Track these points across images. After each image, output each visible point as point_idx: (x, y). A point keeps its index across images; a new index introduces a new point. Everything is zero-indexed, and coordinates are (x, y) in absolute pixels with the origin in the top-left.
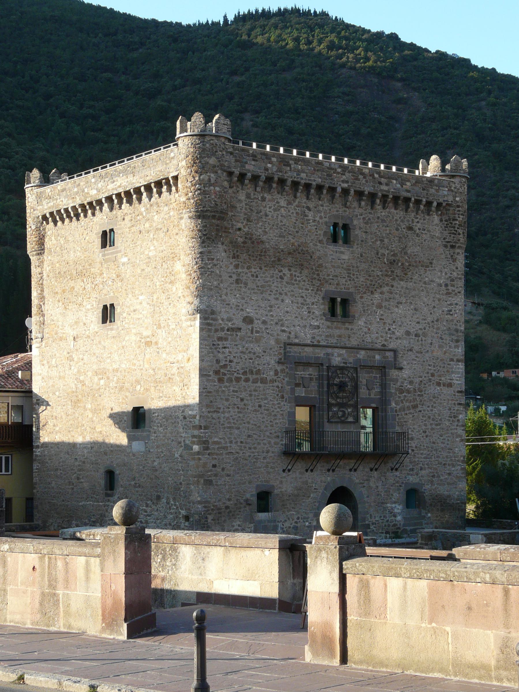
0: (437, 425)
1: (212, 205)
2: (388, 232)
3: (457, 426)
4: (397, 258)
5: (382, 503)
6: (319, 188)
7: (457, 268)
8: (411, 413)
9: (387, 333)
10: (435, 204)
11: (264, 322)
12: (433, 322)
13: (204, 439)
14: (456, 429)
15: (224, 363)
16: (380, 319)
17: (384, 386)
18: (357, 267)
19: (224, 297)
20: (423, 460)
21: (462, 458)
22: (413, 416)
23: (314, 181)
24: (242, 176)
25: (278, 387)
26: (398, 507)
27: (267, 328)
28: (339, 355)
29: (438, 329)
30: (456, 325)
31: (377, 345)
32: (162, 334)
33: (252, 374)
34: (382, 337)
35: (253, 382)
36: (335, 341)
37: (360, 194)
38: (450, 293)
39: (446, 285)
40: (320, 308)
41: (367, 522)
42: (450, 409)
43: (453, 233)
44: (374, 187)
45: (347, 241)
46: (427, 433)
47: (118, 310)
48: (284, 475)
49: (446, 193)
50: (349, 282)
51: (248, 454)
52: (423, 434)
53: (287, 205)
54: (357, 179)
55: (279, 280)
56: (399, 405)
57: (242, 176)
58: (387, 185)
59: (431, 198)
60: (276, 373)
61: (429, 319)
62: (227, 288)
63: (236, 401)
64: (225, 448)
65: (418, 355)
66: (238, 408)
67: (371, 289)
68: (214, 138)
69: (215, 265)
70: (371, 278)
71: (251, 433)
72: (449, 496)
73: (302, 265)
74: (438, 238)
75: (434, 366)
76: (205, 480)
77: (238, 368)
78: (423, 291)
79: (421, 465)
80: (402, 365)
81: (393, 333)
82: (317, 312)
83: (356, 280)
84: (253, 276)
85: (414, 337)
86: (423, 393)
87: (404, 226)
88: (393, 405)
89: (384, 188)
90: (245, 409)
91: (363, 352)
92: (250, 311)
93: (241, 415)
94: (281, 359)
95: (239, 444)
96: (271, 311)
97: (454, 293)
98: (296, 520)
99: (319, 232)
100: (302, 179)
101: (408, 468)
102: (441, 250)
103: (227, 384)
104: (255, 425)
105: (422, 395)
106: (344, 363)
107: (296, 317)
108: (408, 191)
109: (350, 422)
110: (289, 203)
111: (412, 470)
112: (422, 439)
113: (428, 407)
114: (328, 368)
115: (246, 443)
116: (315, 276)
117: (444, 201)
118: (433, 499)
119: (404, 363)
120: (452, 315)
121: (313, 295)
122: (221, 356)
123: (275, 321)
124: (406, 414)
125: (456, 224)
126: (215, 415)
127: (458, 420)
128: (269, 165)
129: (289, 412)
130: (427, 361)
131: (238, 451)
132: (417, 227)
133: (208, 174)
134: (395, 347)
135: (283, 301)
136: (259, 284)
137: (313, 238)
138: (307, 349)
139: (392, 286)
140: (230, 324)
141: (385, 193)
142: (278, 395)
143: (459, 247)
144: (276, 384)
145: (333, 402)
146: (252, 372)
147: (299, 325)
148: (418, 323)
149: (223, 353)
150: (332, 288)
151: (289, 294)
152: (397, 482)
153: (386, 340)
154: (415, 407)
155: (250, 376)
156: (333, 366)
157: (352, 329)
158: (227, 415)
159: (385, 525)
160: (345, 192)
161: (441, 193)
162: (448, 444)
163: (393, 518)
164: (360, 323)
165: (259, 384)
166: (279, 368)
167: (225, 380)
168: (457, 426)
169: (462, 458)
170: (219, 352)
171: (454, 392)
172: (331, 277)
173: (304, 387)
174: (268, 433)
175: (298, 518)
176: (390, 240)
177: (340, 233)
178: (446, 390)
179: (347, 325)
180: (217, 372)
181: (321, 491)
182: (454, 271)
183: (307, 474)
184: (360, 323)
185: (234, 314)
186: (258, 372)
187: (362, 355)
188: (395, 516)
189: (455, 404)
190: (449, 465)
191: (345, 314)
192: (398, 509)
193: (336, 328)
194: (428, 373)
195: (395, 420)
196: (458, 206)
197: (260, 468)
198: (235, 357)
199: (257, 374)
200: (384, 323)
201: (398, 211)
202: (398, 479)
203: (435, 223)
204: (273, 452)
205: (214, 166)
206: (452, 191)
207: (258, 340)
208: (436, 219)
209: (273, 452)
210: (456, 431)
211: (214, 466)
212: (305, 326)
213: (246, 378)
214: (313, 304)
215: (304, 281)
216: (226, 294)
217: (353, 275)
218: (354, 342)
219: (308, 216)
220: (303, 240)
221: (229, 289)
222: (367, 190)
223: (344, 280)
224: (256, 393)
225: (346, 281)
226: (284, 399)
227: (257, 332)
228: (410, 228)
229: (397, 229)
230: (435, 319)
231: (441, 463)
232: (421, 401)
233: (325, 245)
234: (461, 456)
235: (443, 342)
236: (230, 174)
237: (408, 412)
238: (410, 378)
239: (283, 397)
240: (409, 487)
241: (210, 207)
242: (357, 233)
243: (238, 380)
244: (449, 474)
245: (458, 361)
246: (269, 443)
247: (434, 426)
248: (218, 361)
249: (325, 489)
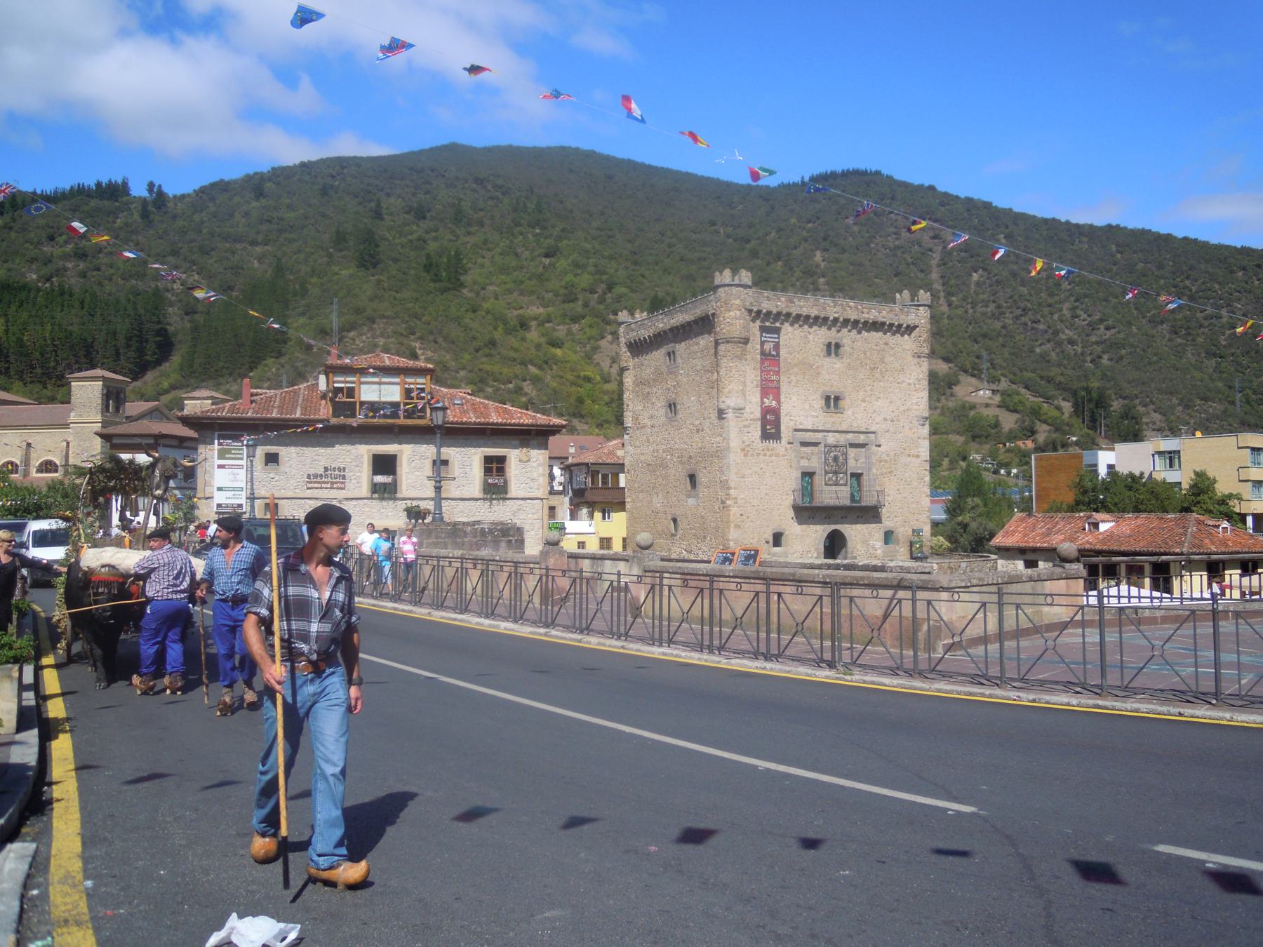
6: (817, 318)
17: (868, 458)
24: (759, 312)
32: (707, 422)
37: (846, 321)
45: (837, 355)
47: (678, 407)
61: (902, 409)
89: (866, 316)
102: (911, 359)
119: (882, 441)
150: (828, 389)
160: (836, 320)
177: (833, 349)
180: (743, 450)
186: (773, 449)
187: (850, 436)
191: (836, 406)
218: (844, 427)
236: (750, 311)
242: (846, 349)
243: (758, 454)
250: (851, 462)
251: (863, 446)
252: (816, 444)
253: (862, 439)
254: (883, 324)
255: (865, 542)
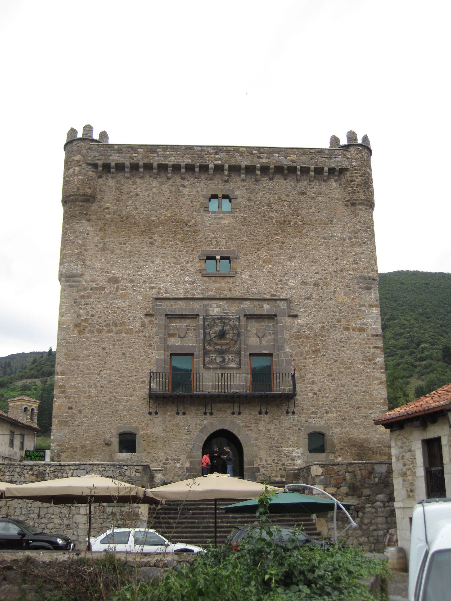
0: (346, 368)
1: (74, 190)
2: (276, 198)
3: (374, 368)
4: (289, 219)
5: (276, 447)
7: (360, 222)
8: (311, 358)
9: (277, 284)
10: (326, 169)
11: (131, 281)
12: (335, 272)
13: (61, 384)
14: (373, 372)
15: (85, 317)
16: (269, 272)
18: (240, 229)
19: (88, 262)
20: (329, 403)
21: (382, 401)
22: (314, 361)
23: (183, 162)
25: (145, 337)
26: (296, 449)
27: (134, 286)
28: (218, 306)
29: (344, 277)
30: (362, 272)
31: (265, 296)
33: (117, 326)
34: (271, 288)
35: (117, 333)
36: (213, 293)
38: (354, 245)
39: (350, 239)
40: (193, 265)
41: (255, 466)
42: (363, 353)
43: (352, 192)
44: (252, 161)
46: (334, 377)
48: (150, 417)
49: (339, 160)
50: (230, 242)
51: (108, 398)
52: (328, 378)
53: (160, 185)
54: (233, 156)
55: (149, 245)
56: (295, 350)
57: (107, 167)
58: (267, 158)
59: (320, 165)
60: (143, 324)
61: (331, 269)
62: (92, 256)
63: (95, 349)
64: (85, 392)
65: (318, 303)
66: (99, 356)
67: (257, 247)
68: (79, 142)
69: (77, 237)
70: (257, 238)
71: (112, 378)
72: (366, 440)
73: (176, 232)
74: (337, 199)
75: (340, 313)
76: (59, 421)
77: (100, 321)
78: (321, 245)
79: (327, 408)
80: (296, 313)
81: (286, 284)
82: (191, 270)
83: (238, 240)
84: (120, 243)
85: (312, 287)
86: (327, 338)
87: (296, 192)
88: (288, 349)
89: (265, 161)
90: (106, 357)
91: (248, 303)
92: (116, 272)
93: (103, 363)
94: (149, 312)
95: (99, 388)
96: (139, 271)
97: (358, 244)
98: (164, 461)
99: (195, 204)
100: (170, 161)
101: (309, 412)
102: (341, 208)
103: (88, 335)
104: (118, 371)
105: (326, 340)
106: (224, 313)
107: (167, 275)
108: (292, 161)
109: (232, 368)
110: (163, 184)
111: (315, 413)
112: (327, 383)
113: (334, 351)
114: (205, 318)
115: (107, 388)
116: (190, 240)
117: (338, 166)
118: (344, 442)
119: (301, 311)
120: (357, 264)
121: (188, 255)
122: (82, 311)
123: (143, 279)
124: (306, 359)
125: (354, 184)
126: (73, 363)
127: (375, 363)
128: (135, 155)
129: (157, 359)
130: (330, 308)
131: (97, 395)
132: (310, 192)
133: (74, 168)
134: (288, 296)
135: (152, 262)
136: (127, 249)
137: (188, 208)
138: (179, 302)
139: (283, 243)
140: (93, 285)
141: (265, 165)
142: (144, 344)
143: (360, 204)
144: (141, 334)
145: (211, 348)
146: (116, 325)
147: (171, 282)
148: (317, 273)
149: (85, 309)
151: (160, 256)
152: (295, 426)
153: (276, 291)
154: (318, 351)
155: (113, 328)
156: (212, 316)
157: (233, 283)
158: (86, 362)
159: (280, 469)
161: (333, 160)
162: (362, 387)
163: (292, 462)
164: (243, 276)
165: (123, 335)
166: (147, 320)
167: (86, 332)
168: (374, 368)
169: (382, 401)
170: (80, 308)
171: (368, 335)
172: (209, 240)
173: (180, 337)
174: (132, 379)
175: (167, 459)
176: (279, 205)
178: (355, 334)
179: (227, 279)
180: (77, 325)
181: (196, 434)
182: (356, 224)
183: (179, 416)
184: (243, 276)
185: (98, 276)
186: (123, 324)
187: (246, 305)
188: (293, 460)
189: (369, 347)
190: (365, 408)
192: (297, 453)
193: (214, 282)
194: (332, 319)
195: (290, 364)
196: (355, 170)
197: (122, 410)
198: (97, 312)
199: (121, 325)
200: (274, 276)
201: (288, 181)
202: (295, 422)
203: (333, 187)
204: (137, 396)
205: (79, 161)
206: (348, 158)
207: (123, 297)
208: (334, 184)
209: (137, 396)
210: (372, 374)
211: (70, 408)
212: (177, 283)
213: (109, 330)
214: (188, 262)
215: (178, 244)
216: (91, 260)
217: (236, 236)
218: (237, 294)
219: (182, 192)
220: (177, 211)
221: (94, 255)
222: (243, 164)
223: (224, 241)
224: (120, 343)
225: (227, 241)
226: (152, 348)
227: (122, 290)
228: (303, 193)
229: (287, 196)
230: (339, 268)
231: (354, 406)
232: (324, 346)
233: (202, 213)
234: (381, 399)
235: (350, 290)
237: (307, 357)
238: (309, 324)
239: (150, 345)
240: (312, 431)
241: (73, 192)
243: (100, 331)
244: (366, 417)
245: (371, 306)
246: (134, 387)
247: (342, 370)
248: (79, 316)
249: (201, 431)
250: (253, 341)
251: (272, 317)
252: (195, 316)
253: (266, 308)
254: (292, 170)
255: (274, 448)
